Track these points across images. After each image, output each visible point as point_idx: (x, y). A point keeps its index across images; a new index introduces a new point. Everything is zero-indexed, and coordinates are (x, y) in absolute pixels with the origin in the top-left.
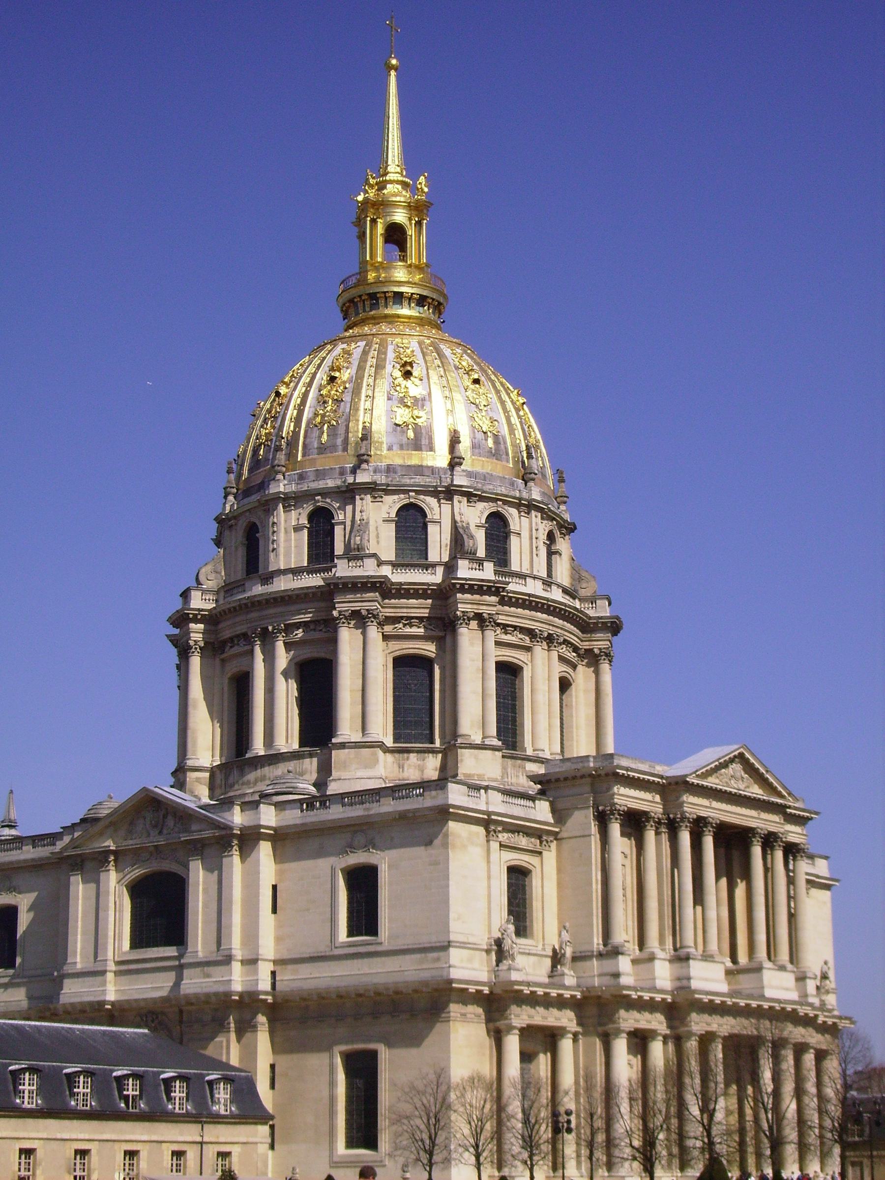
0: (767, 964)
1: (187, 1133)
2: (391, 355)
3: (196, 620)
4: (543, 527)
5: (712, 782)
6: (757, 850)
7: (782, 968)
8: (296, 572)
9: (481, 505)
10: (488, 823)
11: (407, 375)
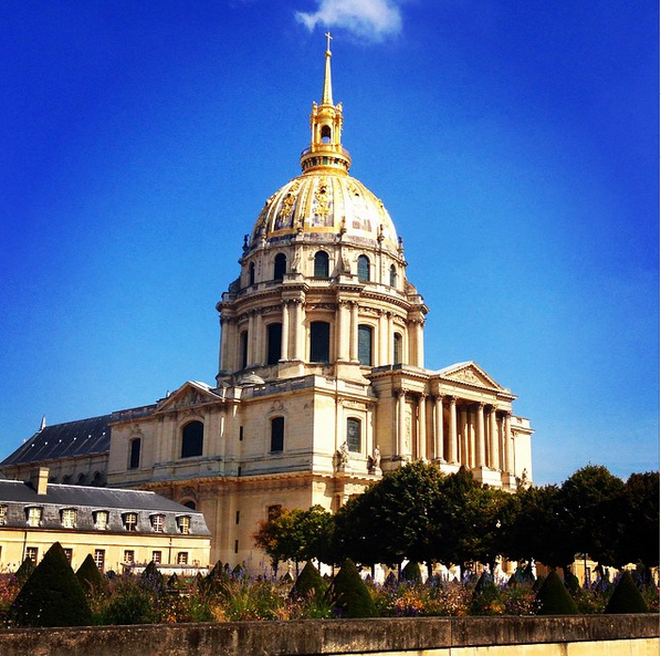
0: (484, 468)
1: (164, 542)
3: (226, 307)
4: (388, 263)
5: (454, 378)
6: (481, 413)
7: (494, 470)
8: (268, 283)
9: (355, 252)
10: (337, 397)
11: (323, 192)
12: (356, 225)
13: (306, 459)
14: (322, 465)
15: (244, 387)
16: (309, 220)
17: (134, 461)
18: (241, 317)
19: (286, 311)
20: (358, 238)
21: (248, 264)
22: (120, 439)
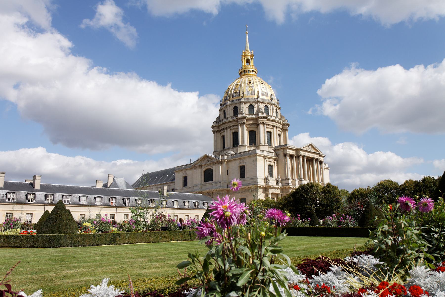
3: (215, 126)
4: (275, 108)
5: (305, 149)
6: (315, 162)
8: (232, 117)
10: (264, 157)
12: (263, 95)
13: (254, 180)
14: (261, 183)
15: (228, 155)
16: (246, 93)
17: (185, 184)
19: (240, 127)
20: (264, 99)
21: (223, 111)
22: (179, 177)
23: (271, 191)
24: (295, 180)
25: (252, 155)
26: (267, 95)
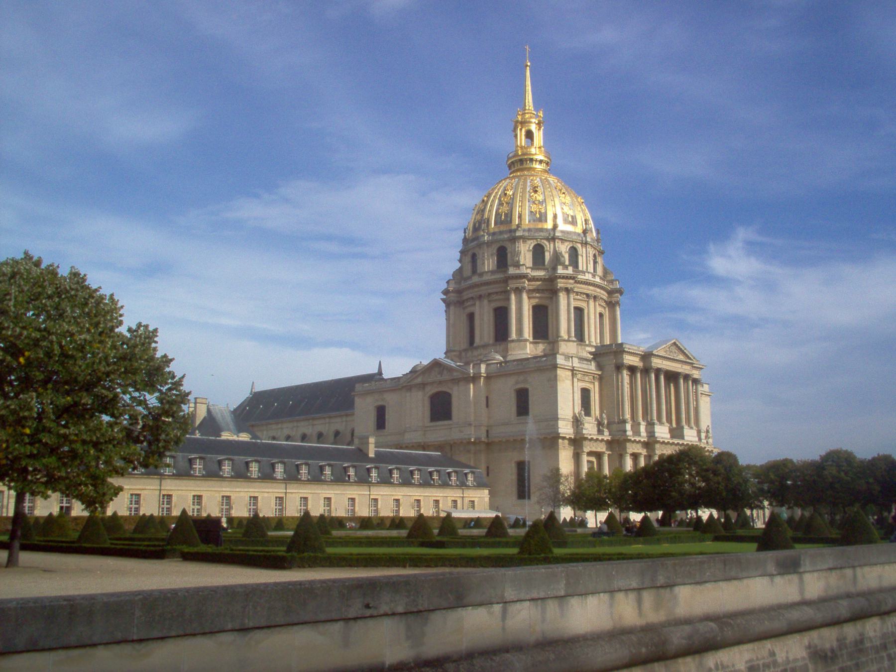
0: (686, 427)
2: (529, 184)
4: (591, 251)
5: (662, 353)
6: (682, 381)
8: (493, 272)
9: (566, 244)
11: (536, 192)
12: (566, 221)
14: (565, 429)
17: (381, 423)
18: (467, 300)
19: (513, 297)
20: (568, 233)
23: (587, 447)
24: (639, 424)
25: (546, 366)
26: (574, 222)
